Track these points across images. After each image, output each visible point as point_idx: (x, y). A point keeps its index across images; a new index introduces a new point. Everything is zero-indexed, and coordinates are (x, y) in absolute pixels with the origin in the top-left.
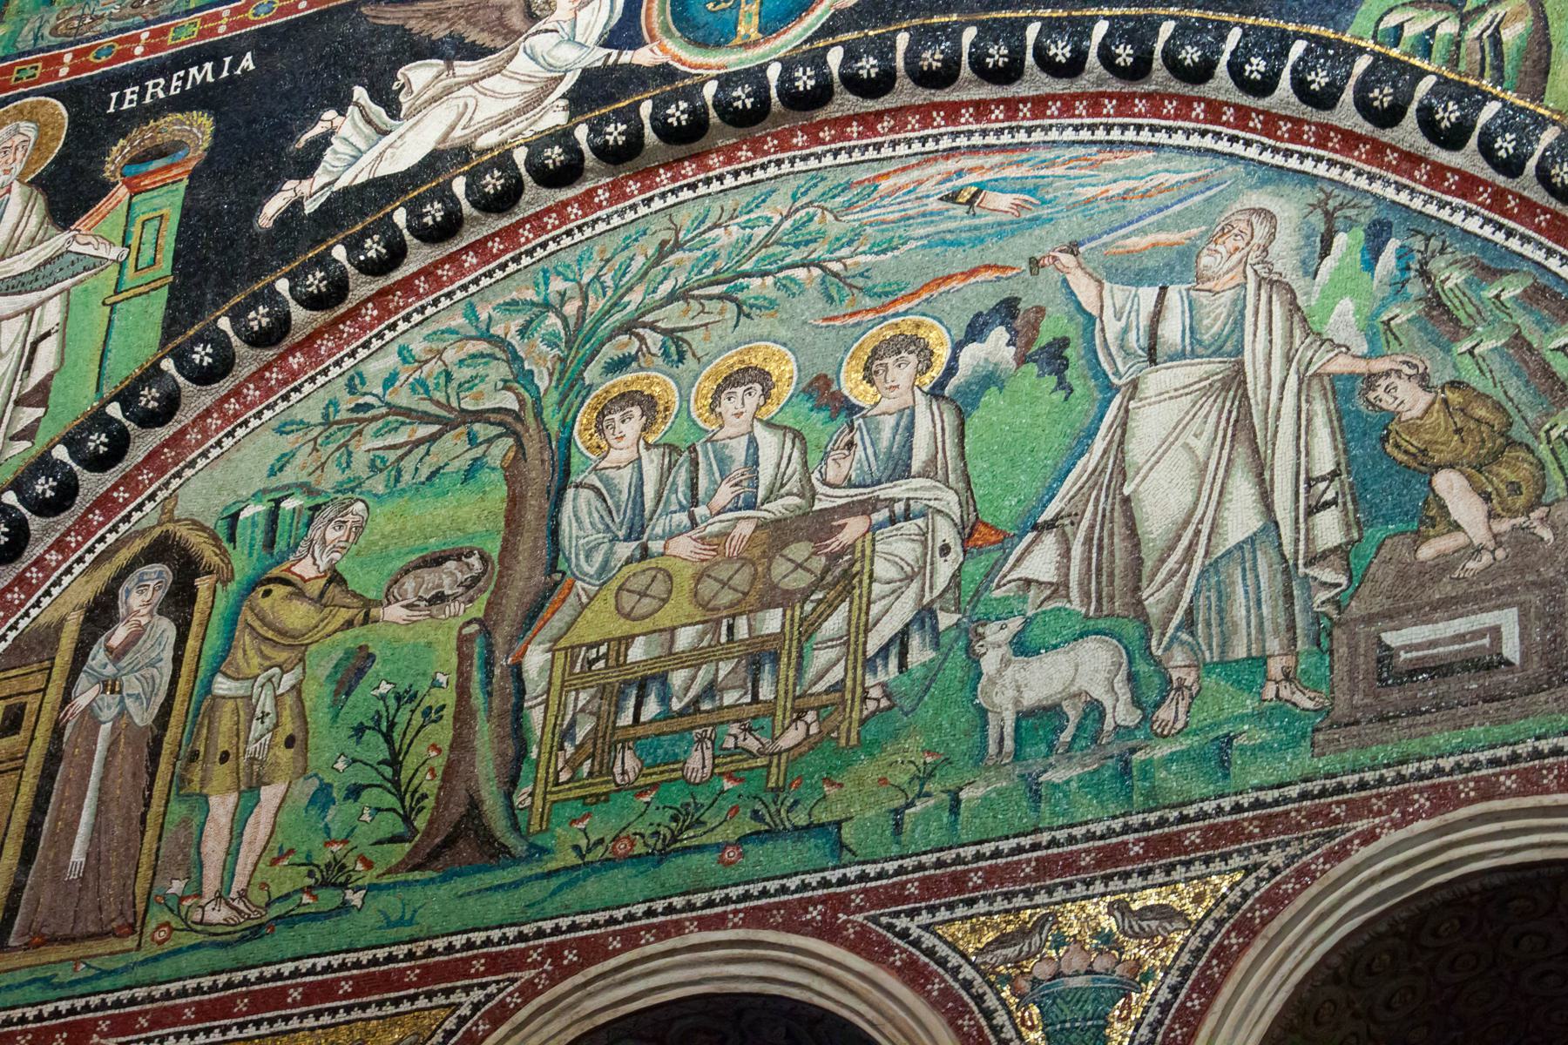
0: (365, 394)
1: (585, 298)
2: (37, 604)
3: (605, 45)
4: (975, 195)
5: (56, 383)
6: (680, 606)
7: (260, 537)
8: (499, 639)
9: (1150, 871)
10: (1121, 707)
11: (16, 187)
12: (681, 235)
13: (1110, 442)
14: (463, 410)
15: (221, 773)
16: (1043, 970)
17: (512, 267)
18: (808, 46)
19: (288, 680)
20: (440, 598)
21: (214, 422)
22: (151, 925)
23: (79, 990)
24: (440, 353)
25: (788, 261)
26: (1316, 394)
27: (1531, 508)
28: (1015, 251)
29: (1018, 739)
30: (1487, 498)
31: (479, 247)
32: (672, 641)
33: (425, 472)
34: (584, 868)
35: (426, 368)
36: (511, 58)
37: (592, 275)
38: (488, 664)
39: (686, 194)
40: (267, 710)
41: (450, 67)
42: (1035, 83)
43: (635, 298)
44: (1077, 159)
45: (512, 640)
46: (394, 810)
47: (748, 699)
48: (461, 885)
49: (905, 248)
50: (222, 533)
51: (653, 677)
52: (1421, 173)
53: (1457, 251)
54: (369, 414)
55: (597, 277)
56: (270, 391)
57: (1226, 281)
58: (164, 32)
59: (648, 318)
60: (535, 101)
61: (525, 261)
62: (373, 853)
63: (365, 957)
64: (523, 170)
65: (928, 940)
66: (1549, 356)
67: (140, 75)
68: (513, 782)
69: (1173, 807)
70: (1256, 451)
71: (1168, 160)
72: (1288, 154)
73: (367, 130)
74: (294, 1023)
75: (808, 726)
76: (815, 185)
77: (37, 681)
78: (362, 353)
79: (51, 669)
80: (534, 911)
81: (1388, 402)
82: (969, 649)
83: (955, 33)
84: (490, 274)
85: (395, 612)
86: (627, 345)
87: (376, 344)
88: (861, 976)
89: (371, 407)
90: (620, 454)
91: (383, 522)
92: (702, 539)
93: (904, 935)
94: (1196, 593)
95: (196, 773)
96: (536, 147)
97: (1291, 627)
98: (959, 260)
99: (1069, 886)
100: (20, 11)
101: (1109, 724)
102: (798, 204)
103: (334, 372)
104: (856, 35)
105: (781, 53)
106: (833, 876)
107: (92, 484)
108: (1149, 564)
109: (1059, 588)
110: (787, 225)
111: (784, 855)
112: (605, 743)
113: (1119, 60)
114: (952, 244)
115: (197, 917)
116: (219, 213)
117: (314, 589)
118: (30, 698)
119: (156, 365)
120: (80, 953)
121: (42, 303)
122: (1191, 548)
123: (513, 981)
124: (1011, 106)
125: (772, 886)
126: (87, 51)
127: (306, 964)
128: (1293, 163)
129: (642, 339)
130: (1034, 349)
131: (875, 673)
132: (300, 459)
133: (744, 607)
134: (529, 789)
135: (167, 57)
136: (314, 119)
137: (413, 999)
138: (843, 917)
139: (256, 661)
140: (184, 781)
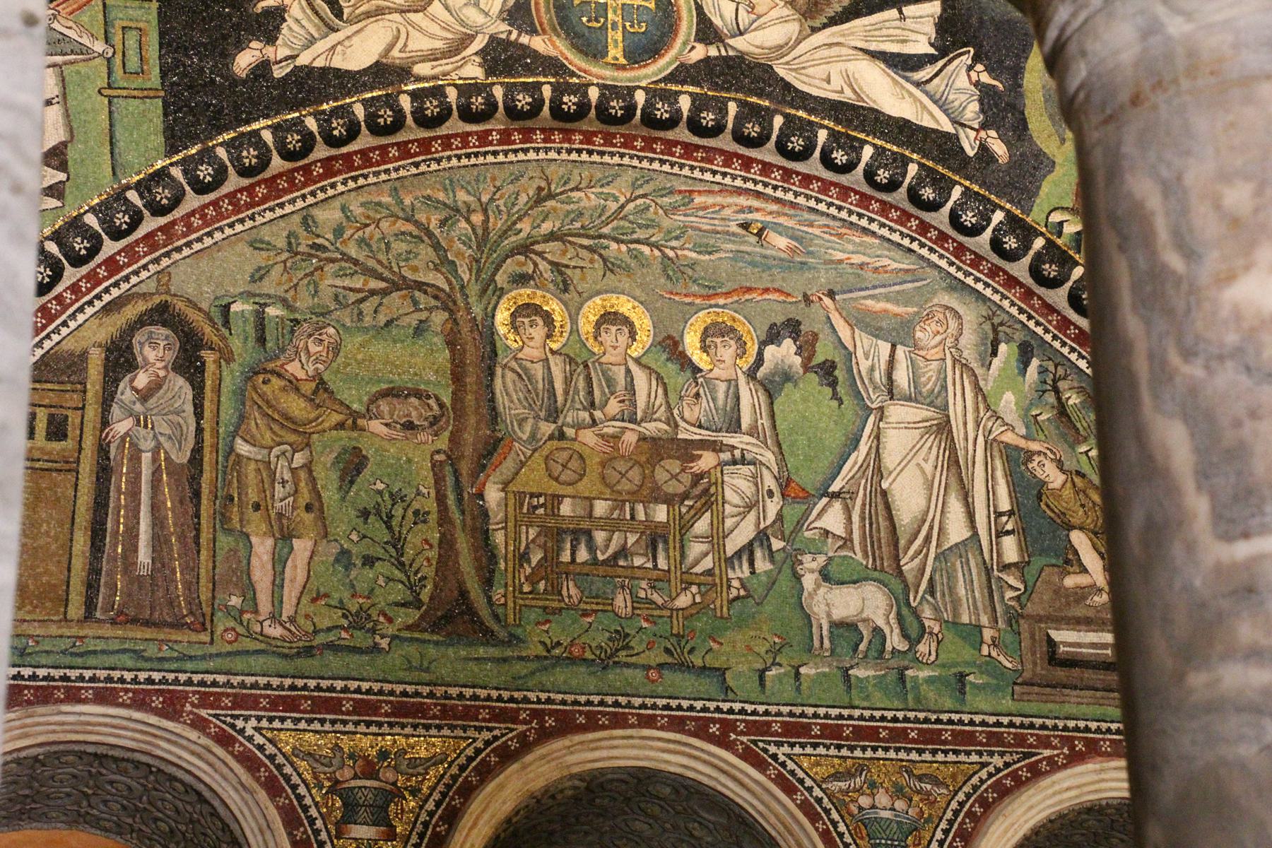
0: (318, 236)
5: (72, 154)
12: (553, 187)
13: (870, 448)
14: (404, 278)
16: (864, 801)
17: (423, 168)
19: (299, 459)
21: (196, 222)
22: (220, 629)
23: (166, 666)
25: (635, 236)
26: (996, 454)
28: (796, 284)
31: (403, 146)
32: (591, 506)
33: (382, 319)
35: (368, 230)
37: (488, 197)
40: (286, 478)
42: (813, 165)
43: (525, 226)
44: (828, 226)
45: (474, 475)
46: (402, 582)
47: (650, 565)
48: (463, 653)
49: (717, 255)
55: (492, 200)
57: (934, 354)
59: (537, 247)
63: (399, 688)
68: (488, 583)
69: (935, 712)
70: (961, 480)
71: (889, 250)
72: (967, 274)
73: (317, 20)
74: (350, 727)
75: (694, 596)
76: (647, 182)
79: (85, 392)
80: (517, 683)
81: (1039, 473)
85: (376, 426)
88: (756, 781)
92: (602, 436)
93: (775, 757)
94: (934, 570)
97: (994, 610)
99: (875, 749)
101: (889, 647)
104: (698, 90)
105: (643, 84)
106: (725, 706)
107: (110, 247)
108: (902, 543)
109: (847, 542)
112: (552, 570)
113: (878, 179)
117: (308, 388)
118: (69, 413)
120: (161, 636)
122: (928, 539)
123: (512, 730)
124: (787, 174)
125: (685, 704)
127: (353, 685)
128: (970, 281)
129: (536, 265)
131: (734, 569)
134: (502, 591)
138: (733, 736)
139: (268, 435)
140: (225, 519)
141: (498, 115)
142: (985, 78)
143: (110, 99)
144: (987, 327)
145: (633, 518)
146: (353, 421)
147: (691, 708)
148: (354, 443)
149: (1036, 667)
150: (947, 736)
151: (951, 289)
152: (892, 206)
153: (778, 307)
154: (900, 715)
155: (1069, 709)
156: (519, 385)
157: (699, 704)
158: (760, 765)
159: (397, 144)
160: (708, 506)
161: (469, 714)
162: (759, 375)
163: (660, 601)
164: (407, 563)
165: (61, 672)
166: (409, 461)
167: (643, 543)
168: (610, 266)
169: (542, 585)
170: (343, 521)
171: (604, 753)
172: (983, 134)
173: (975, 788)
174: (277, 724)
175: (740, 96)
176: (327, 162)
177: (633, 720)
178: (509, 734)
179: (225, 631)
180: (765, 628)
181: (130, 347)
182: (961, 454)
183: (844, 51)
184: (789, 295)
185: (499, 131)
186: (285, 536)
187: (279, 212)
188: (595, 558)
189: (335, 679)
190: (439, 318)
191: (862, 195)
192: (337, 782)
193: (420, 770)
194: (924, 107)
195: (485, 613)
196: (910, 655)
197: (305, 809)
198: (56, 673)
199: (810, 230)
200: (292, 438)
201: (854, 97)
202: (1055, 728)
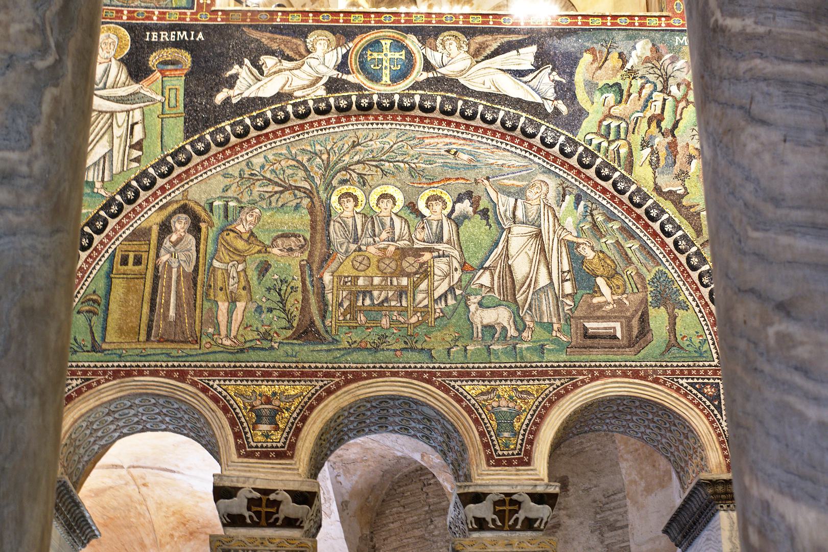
1: (329, 155)
2: (139, 219)
5: (145, 143)
14: (290, 185)
15: (221, 295)
16: (495, 404)
17: (301, 137)
18: (407, 91)
19: (241, 267)
21: (200, 168)
22: (204, 342)
23: (180, 359)
25: (397, 159)
28: (471, 175)
29: (483, 334)
31: (292, 128)
32: (372, 280)
33: (280, 204)
35: (275, 166)
36: (303, 65)
38: (311, 276)
39: (360, 126)
42: (478, 122)
43: (347, 159)
47: (399, 305)
48: (311, 348)
49: (435, 165)
51: (368, 292)
52: (591, 182)
54: (256, 178)
55: (332, 148)
56: (219, 161)
57: (537, 202)
59: (352, 167)
60: (313, 84)
63: (282, 365)
66: (626, 249)
67: (158, 28)
70: (546, 259)
72: (551, 165)
73: (252, 77)
74: (260, 383)
77: (146, 248)
80: (336, 360)
81: (583, 253)
82: (466, 303)
84: (294, 137)
85: (275, 251)
89: (257, 175)
92: (379, 249)
93: (453, 387)
94: (532, 299)
97: (559, 315)
99: (501, 381)
101: (509, 335)
102: (399, 140)
106: (431, 365)
107: (160, 182)
108: (517, 287)
109: (491, 289)
111: (415, 356)
115: (220, 342)
117: (245, 236)
118: (143, 254)
119: (183, 147)
120: (179, 347)
121: (133, 110)
122: (529, 286)
124: (468, 127)
126: (134, 12)
127: (261, 364)
128: (553, 168)
129: (350, 175)
132: (233, 188)
133: (395, 274)
135: (167, 24)
136: (231, 66)
139: (227, 257)
140: (207, 295)
141: (332, 111)
142: (557, 78)
143: (162, 119)
144: (560, 189)
145: (391, 283)
146: (265, 249)
147: (415, 367)
148: (265, 259)
149: (578, 340)
150: (535, 373)
151: (544, 172)
152: (515, 137)
153: (462, 186)
154: (513, 365)
155: (593, 357)
157: (419, 365)
158: (447, 391)
159: (289, 127)
160: (426, 276)
161: (314, 374)
162: (453, 217)
163: (403, 321)
164: (287, 310)
165: (136, 364)
166: (289, 265)
167: (396, 296)
168: (385, 173)
169: (348, 316)
170: (259, 293)
171: (374, 389)
172: (555, 102)
173: (547, 395)
174: (227, 382)
175: (443, 93)
176: (257, 137)
177: (388, 374)
178: (331, 383)
180: (452, 329)
181: (170, 223)
182: (546, 246)
185: (335, 118)
186: (233, 301)
187: (236, 161)
188: (373, 303)
189: (253, 362)
190: (306, 202)
191: (502, 133)
192: (254, 406)
193: (291, 400)
195: (322, 331)
196: (519, 338)
197: (239, 418)
198: (134, 364)
200: (237, 258)
201: (496, 90)
202: (585, 366)
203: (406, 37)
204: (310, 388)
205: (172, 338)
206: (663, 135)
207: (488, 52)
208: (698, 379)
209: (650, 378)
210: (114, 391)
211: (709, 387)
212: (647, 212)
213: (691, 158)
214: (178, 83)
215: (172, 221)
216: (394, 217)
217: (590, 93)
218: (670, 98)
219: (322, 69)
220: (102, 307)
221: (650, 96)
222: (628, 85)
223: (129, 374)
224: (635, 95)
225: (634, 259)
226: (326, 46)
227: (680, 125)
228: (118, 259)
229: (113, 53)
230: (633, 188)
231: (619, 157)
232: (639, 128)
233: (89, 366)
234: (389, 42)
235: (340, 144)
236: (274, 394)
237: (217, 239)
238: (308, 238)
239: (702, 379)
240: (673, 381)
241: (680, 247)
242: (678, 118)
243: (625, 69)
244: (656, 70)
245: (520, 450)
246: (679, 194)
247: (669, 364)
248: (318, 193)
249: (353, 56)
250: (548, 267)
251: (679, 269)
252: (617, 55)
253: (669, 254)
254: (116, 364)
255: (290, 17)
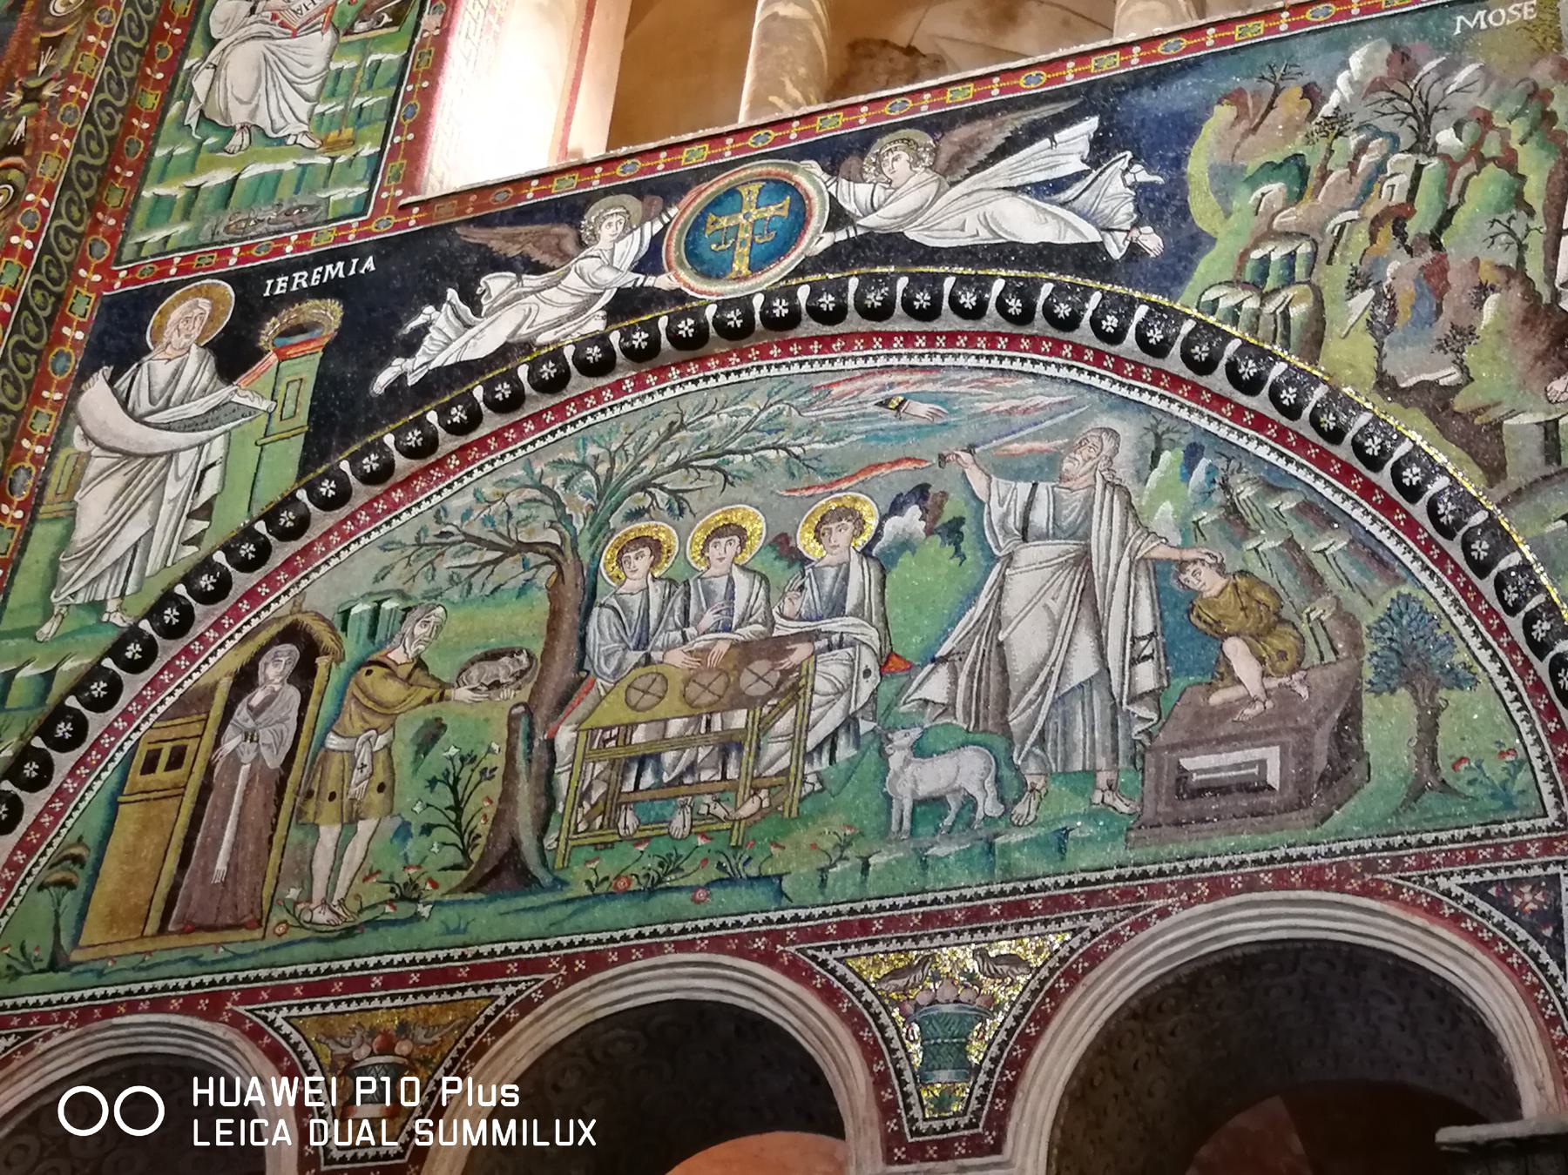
1: (613, 462)
3: (636, 270)
4: (902, 403)
5: (217, 504)
6: (672, 702)
7: (365, 629)
8: (539, 720)
9: (1005, 927)
10: (989, 802)
11: (194, 348)
16: (923, 998)
17: (560, 434)
19: (382, 740)
20: (496, 685)
21: (334, 538)
22: (274, 920)
23: (219, 967)
24: (504, 496)
25: (763, 444)
27: (1293, 671)
29: (913, 821)
30: (1262, 661)
31: (536, 417)
33: (489, 587)
34: (597, 895)
35: (493, 507)
36: (564, 276)
38: (530, 737)
39: (691, 387)
41: (519, 279)
42: (948, 321)
43: (649, 465)
47: (718, 777)
48: (502, 905)
49: (847, 440)
50: (338, 624)
51: (651, 756)
53: (1249, 470)
54: (451, 539)
55: (622, 446)
58: (308, 235)
59: (658, 481)
60: (581, 310)
61: (570, 430)
62: (439, 877)
63: (430, 956)
64: (570, 363)
65: (841, 969)
66: (1312, 556)
67: (289, 268)
68: (543, 829)
70: (1096, 613)
71: (1044, 386)
72: (1131, 387)
73: (457, 323)
74: (376, 1003)
77: (196, 729)
78: (447, 493)
79: (206, 720)
80: (556, 927)
81: (1194, 583)
83: (891, 281)
84: (543, 438)
85: (463, 693)
86: (641, 500)
87: (457, 486)
89: (451, 534)
90: (632, 584)
91: (457, 624)
93: (823, 964)
94: (1048, 719)
95: (311, 807)
96: (580, 346)
97: (1115, 750)
98: (888, 452)
99: (945, 935)
100: (202, 212)
101: (979, 815)
103: (425, 505)
105: (764, 287)
106: (775, 916)
107: (242, 581)
108: (1014, 694)
109: (948, 708)
110: (764, 415)
111: (740, 897)
112: (613, 804)
114: (883, 439)
115: (307, 917)
116: (344, 380)
117: (403, 672)
119: (293, 494)
121: (210, 440)
123: (537, 981)
124: (931, 337)
125: (730, 921)
126: (250, 247)
127: (385, 959)
128: (1134, 395)
129: (653, 496)
130: (939, 524)
131: (811, 763)
132: (400, 568)
134: (555, 835)
136: (418, 312)
137: (463, 990)
138: (779, 948)
139: (358, 724)
142: (1143, 176)
148: (437, 715)
150: (1038, 904)
156: (615, 620)
166: (487, 720)
169: (599, 821)
172: (1135, 233)
174: (306, 1011)
179: (279, 924)
183: (984, 195)
184: (921, 461)
186: (350, 820)
194: (1068, 224)
199: (957, 389)
200: (378, 721)
203: (795, 169)
204: (485, 1003)
205: (210, 921)
206: (1410, 251)
207: (981, 155)
208: (1494, 871)
209: (1355, 884)
210: (73, 1056)
211: (1526, 889)
212: (1358, 448)
213: (1483, 290)
214: (305, 368)
215: (261, 664)
216: (737, 573)
217: (1224, 196)
218: (1435, 161)
219: (607, 276)
220: (88, 870)
221: (1380, 168)
222: (1322, 153)
223: (109, 1011)
224: (1338, 173)
225: (1331, 578)
226: (620, 227)
227: (1459, 219)
228: (139, 760)
229: (195, 333)
230: (1320, 392)
231: (1287, 326)
232: (1346, 247)
233: (37, 1005)
234: (755, 188)
235: (639, 433)
236: (404, 1028)
237: (346, 685)
238: (538, 655)
239: (1508, 869)
240: (1422, 883)
241: (1443, 520)
242: (1453, 200)
243: (1319, 119)
244: (1397, 103)
245: (977, 1114)
246: (1445, 387)
247: (1412, 840)
248: (574, 549)
249: (676, 233)
250: (1098, 632)
251: (1456, 584)
252: (1298, 92)
253: (1426, 550)
254: (88, 993)
255: (555, 184)
